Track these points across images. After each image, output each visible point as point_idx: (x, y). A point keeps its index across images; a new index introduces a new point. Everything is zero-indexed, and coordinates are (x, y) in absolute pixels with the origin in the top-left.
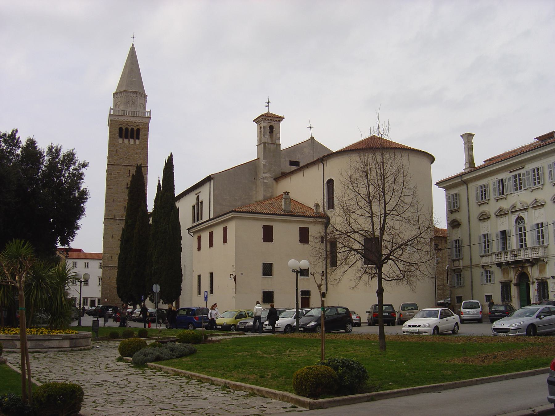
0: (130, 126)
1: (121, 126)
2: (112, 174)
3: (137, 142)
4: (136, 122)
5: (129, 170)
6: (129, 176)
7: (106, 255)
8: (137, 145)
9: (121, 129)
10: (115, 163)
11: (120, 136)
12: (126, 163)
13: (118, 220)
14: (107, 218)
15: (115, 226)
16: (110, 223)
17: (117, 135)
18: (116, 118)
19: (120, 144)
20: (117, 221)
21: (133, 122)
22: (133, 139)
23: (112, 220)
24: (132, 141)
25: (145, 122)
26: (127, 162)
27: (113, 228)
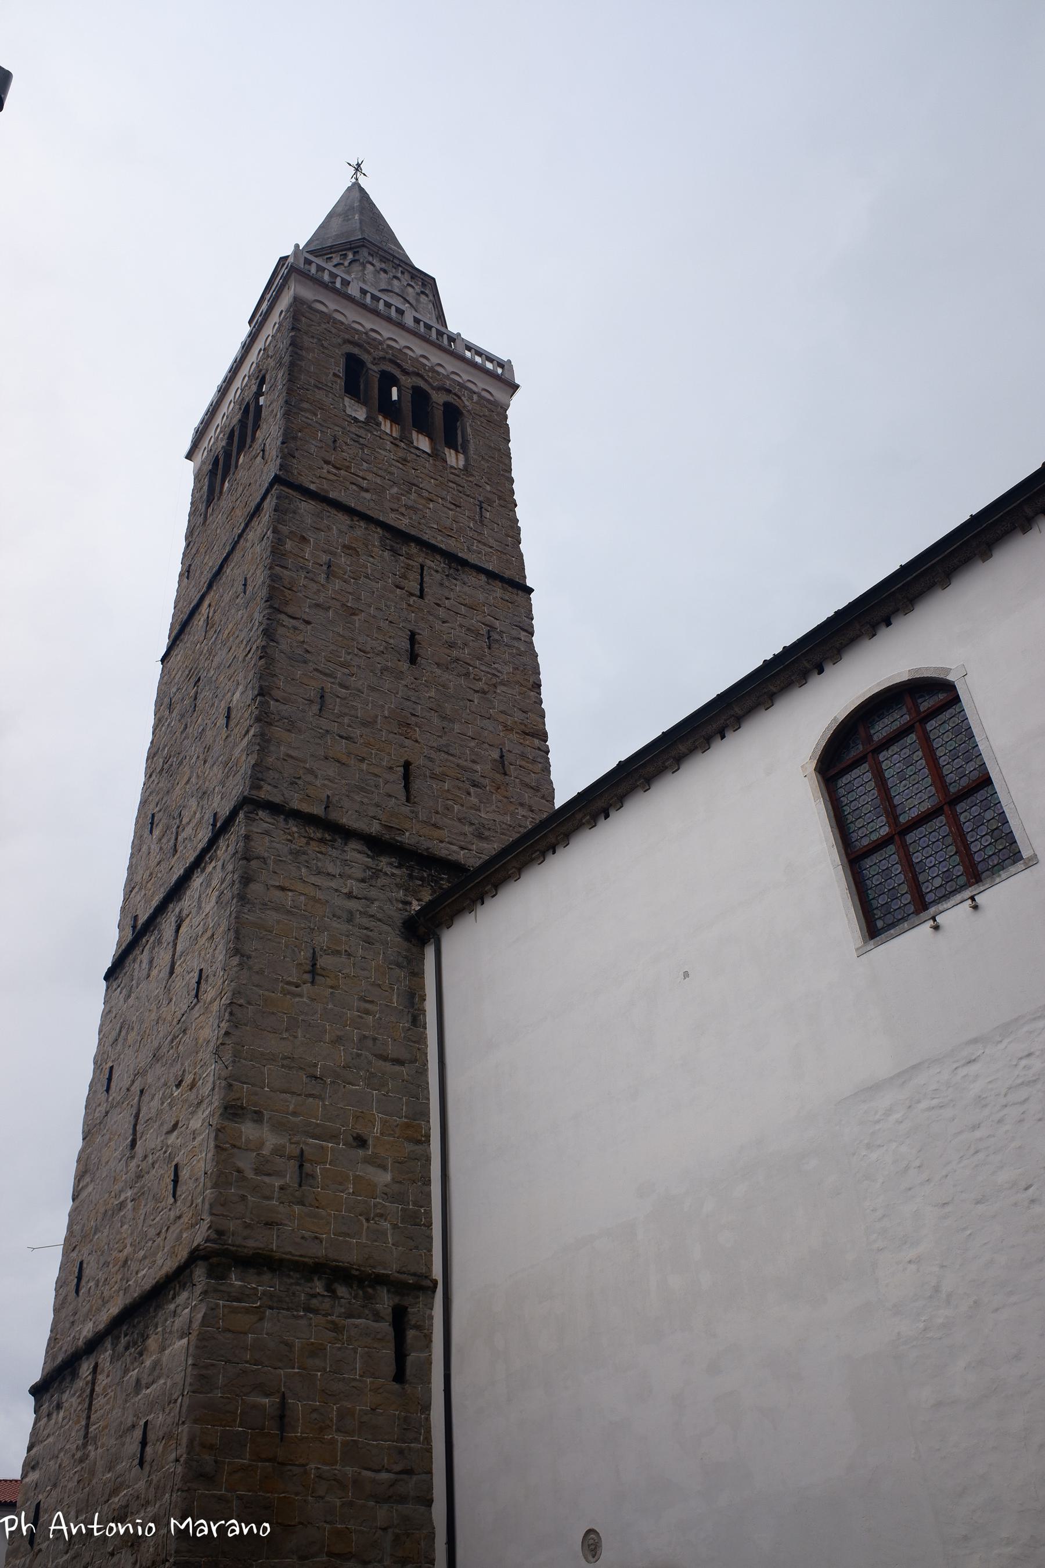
3: (454, 459)
4: (438, 373)
6: (421, 596)
7: (248, 1130)
8: (452, 467)
9: (354, 367)
11: (353, 387)
13: (354, 845)
15: (333, 884)
16: (296, 854)
17: (335, 375)
19: (356, 420)
20: (355, 854)
24: (423, 443)
25: (485, 394)
27: (319, 895)
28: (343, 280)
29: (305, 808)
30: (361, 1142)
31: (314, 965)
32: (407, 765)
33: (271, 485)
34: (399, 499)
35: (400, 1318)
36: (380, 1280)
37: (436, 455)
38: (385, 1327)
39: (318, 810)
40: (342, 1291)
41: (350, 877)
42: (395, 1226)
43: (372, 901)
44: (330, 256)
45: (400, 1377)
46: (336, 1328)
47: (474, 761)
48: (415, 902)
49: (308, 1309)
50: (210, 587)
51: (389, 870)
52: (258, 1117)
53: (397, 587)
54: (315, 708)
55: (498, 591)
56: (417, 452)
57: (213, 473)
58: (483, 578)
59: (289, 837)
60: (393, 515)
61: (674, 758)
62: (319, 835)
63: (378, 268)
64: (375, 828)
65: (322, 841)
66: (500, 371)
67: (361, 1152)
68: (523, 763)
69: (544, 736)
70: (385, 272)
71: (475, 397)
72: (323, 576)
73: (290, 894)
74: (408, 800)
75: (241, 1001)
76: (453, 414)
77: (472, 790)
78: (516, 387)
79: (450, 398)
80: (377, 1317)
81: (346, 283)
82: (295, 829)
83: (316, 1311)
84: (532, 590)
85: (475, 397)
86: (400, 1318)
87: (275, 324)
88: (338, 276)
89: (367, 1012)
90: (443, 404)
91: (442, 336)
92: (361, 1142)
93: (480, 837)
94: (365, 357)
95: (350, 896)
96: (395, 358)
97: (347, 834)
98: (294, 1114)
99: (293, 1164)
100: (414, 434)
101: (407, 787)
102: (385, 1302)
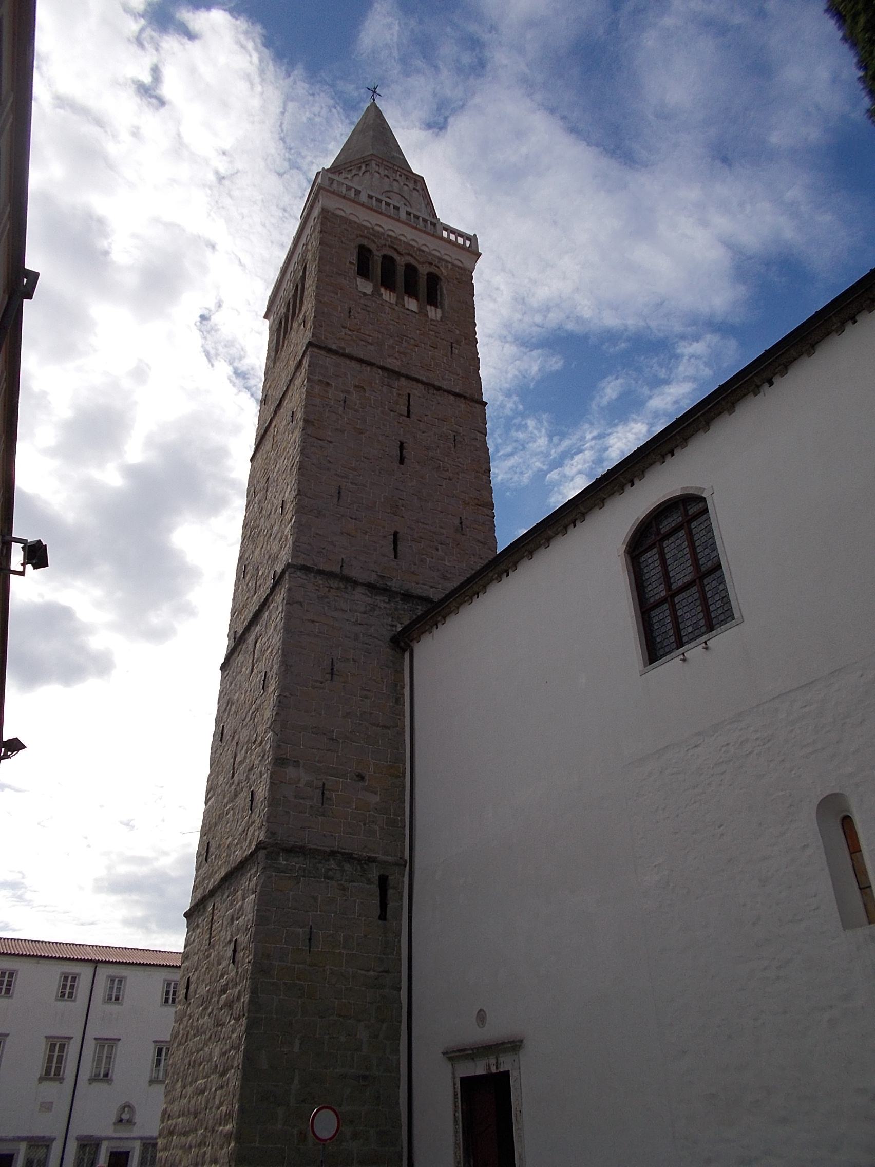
0: (399, 253)
1: (365, 242)
2: (328, 384)
3: (433, 313)
4: (423, 251)
5: (409, 395)
6: (408, 416)
8: (432, 320)
9: (364, 254)
10: (344, 349)
11: (363, 271)
12: (393, 363)
13: (360, 589)
14: (305, 569)
17: (350, 263)
18: (347, 210)
19: (365, 294)
20: (360, 596)
21: (413, 247)
22: (417, 300)
23: (335, 583)
24: (412, 304)
25: (456, 262)
26: (399, 363)
28: (356, 190)
29: (327, 568)
30: (361, 777)
31: (332, 669)
32: (396, 534)
33: (307, 348)
34: (394, 348)
35: (383, 882)
36: (372, 860)
37: (422, 312)
38: (375, 888)
39: (336, 569)
40: (347, 867)
41: (356, 611)
42: (381, 828)
43: (371, 625)
44: (350, 168)
45: (383, 917)
46: (344, 889)
47: (441, 527)
48: (399, 625)
49: (326, 878)
50: (275, 413)
51: (382, 605)
52: (297, 764)
53: (392, 411)
54: (335, 500)
55: (462, 405)
56: (408, 312)
57: (279, 330)
58: (452, 398)
59: (317, 588)
60: (389, 360)
61: (546, 539)
62: (336, 585)
63: (383, 175)
64: (373, 578)
65: (338, 589)
66: (468, 243)
67: (361, 784)
68: (476, 526)
69: (491, 506)
70: (388, 177)
71: (450, 266)
72: (341, 408)
73: (317, 624)
74: (396, 557)
75: (287, 694)
76: (433, 280)
77: (439, 547)
78: (480, 254)
79: (433, 269)
80: (369, 882)
81: (358, 192)
82: (321, 582)
83: (332, 879)
84: (486, 403)
85: (450, 266)
86: (383, 882)
87: (315, 218)
88: (352, 188)
89: (367, 697)
90: (428, 274)
91: (427, 222)
92: (361, 777)
93: (444, 578)
94: (373, 247)
95: (356, 623)
96: (394, 243)
97: (355, 583)
98: (319, 762)
99: (319, 792)
100: (406, 298)
101: (395, 549)
102: (374, 873)
